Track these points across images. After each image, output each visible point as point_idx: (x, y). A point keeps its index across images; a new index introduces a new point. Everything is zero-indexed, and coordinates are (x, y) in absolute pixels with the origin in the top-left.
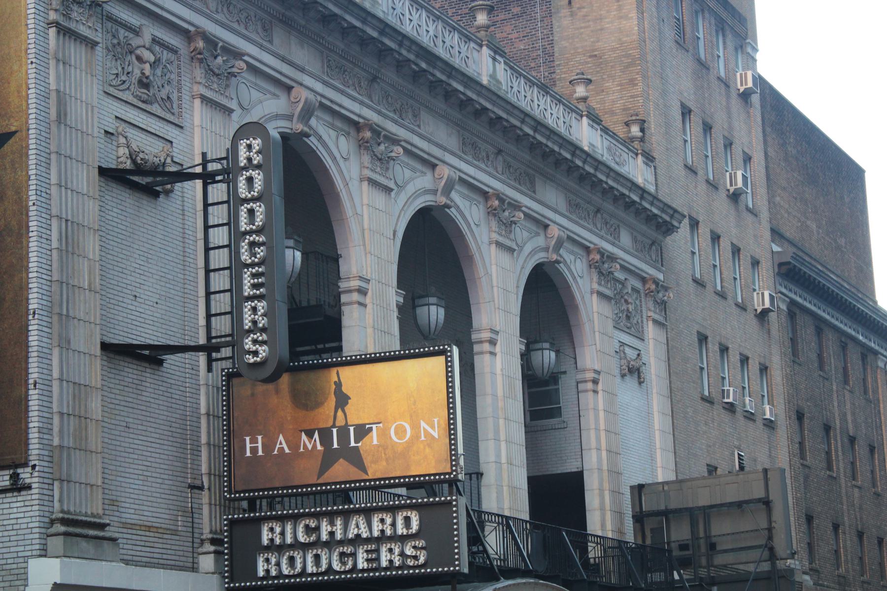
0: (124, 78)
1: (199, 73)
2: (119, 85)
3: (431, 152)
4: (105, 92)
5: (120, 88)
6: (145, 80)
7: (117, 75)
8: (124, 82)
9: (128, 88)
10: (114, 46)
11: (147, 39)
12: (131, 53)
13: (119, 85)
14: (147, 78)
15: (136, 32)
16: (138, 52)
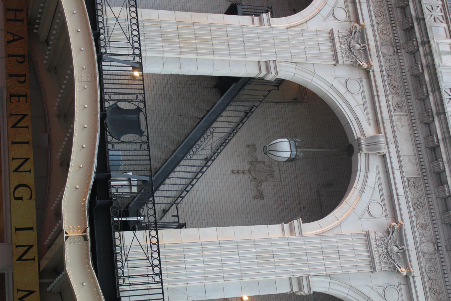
3: (399, 197)
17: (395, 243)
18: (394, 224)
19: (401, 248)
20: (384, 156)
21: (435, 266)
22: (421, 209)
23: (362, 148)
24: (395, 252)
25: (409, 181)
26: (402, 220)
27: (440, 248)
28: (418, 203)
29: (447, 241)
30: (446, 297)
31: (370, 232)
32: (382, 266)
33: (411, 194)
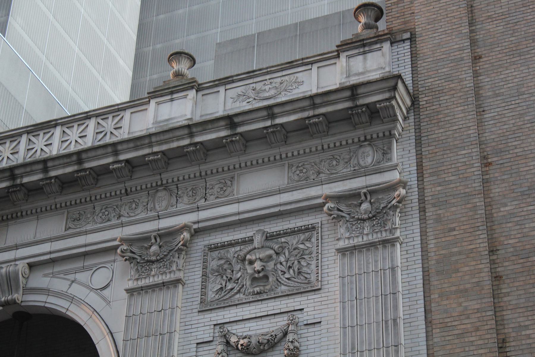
0: (229, 286)
1: (342, 230)
2: (225, 295)
4: (199, 312)
5: (225, 298)
6: (256, 275)
7: (222, 288)
8: (232, 289)
9: (239, 292)
10: (221, 266)
11: (258, 241)
12: (243, 260)
13: (225, 295)
14: (259, 272)
15: (251, 240)
16: (248, 257)
17: (356, 206)
18: (325, 208)
19: (363, 198)
20: (31, 266)
21: (188, 190)
22: (109, 209)
23: (12, 299)
24: (370, 206)
25: (70, 228)
26: (115, 240)
27: (369, 137)
28: (298, 172)
29: (193, 163)
30: (90, 205)
31: (338, 247)
32: (175, 269)
33: (89, 225)
